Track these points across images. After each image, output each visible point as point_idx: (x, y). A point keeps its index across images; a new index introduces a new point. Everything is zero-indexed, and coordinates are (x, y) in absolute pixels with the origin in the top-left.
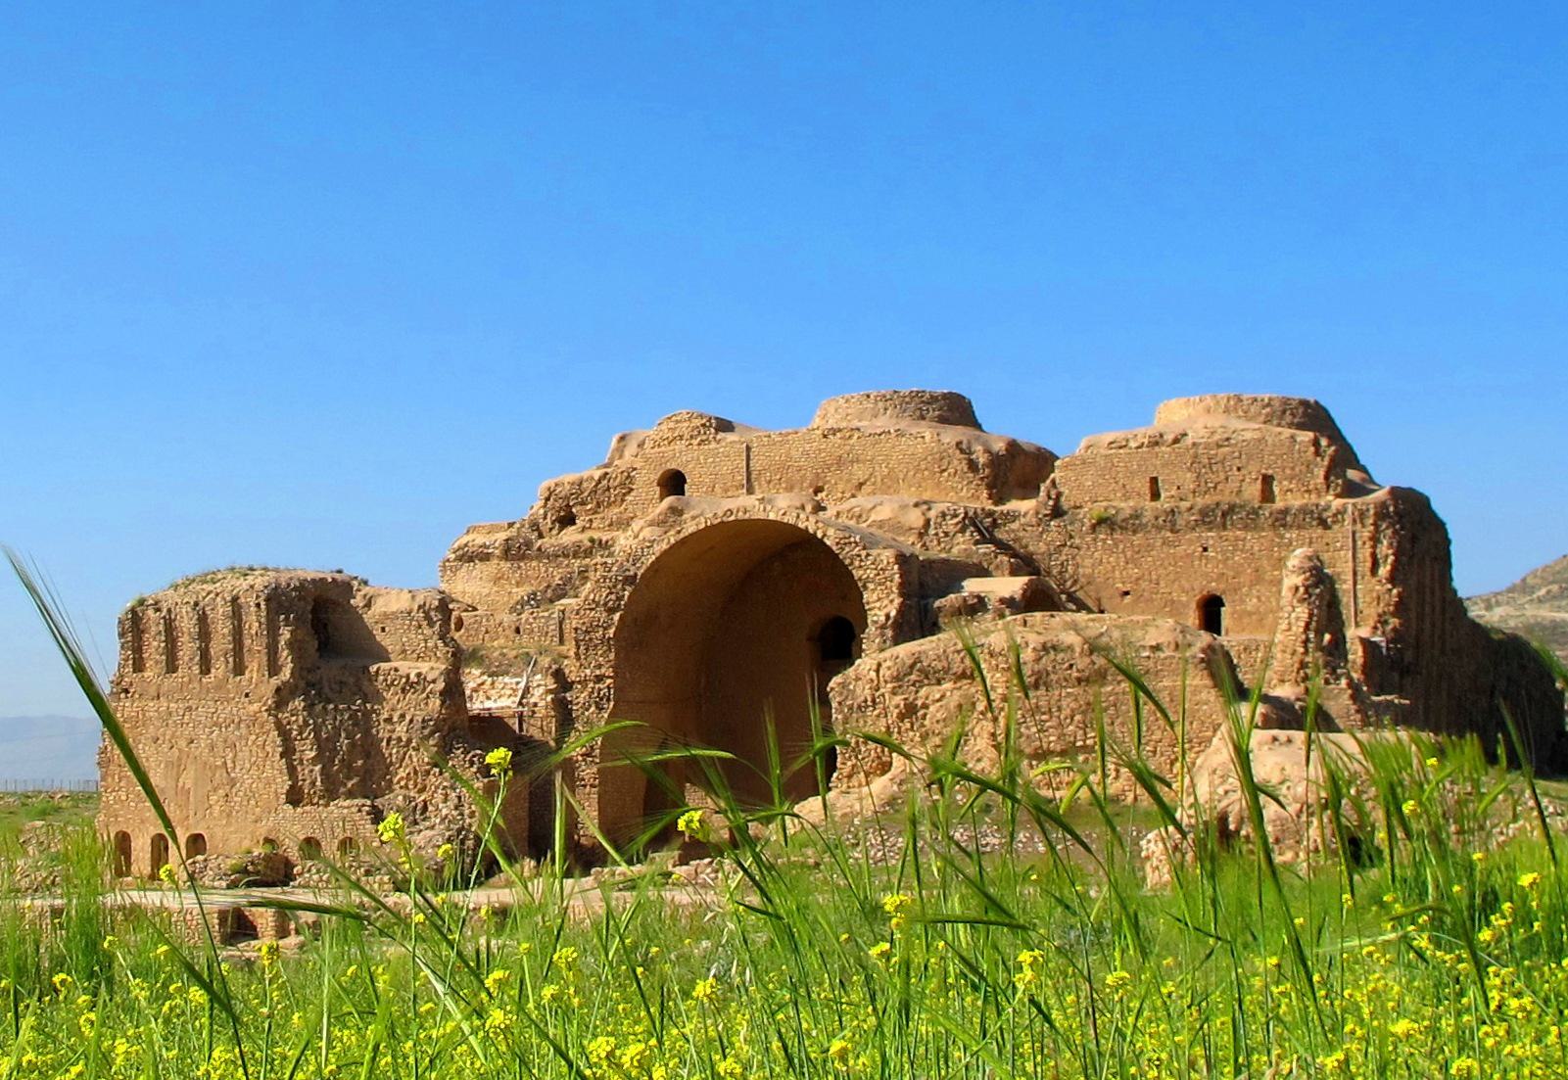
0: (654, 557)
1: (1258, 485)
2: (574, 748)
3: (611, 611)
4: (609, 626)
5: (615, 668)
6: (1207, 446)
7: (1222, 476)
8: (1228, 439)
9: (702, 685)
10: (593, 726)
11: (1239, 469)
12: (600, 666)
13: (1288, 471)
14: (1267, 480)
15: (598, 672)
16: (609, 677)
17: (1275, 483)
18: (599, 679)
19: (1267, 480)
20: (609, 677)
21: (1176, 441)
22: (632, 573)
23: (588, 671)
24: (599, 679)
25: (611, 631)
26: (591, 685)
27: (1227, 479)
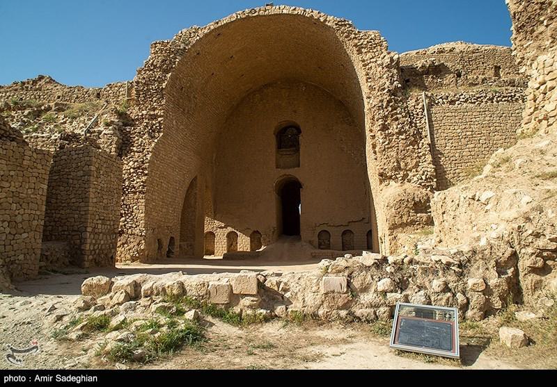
0: (198, 38)
1: (493, 71)
2: (128, 165)
3: (166, 71)
4: (163, 81)
5: (166, 111)
6: (467, 52)
7: (475, 67)
8: (478, 49)
9: (214, 158)
10: (145, 146)
11: (483, 63)
12: (154, 109)
13: (508, 64)
14: (497, 68)
15: (152, 113)
16: (160, 116)
17: (501, 70)
18: (155, 117)
19: (497, 68)
20: (160, 116)
21: (451, 51)
22: (181, 47)
23: (144, 112)
24: (155, 117)
25: (164, 85)
26: (147, 121)
27: (477, 67)
